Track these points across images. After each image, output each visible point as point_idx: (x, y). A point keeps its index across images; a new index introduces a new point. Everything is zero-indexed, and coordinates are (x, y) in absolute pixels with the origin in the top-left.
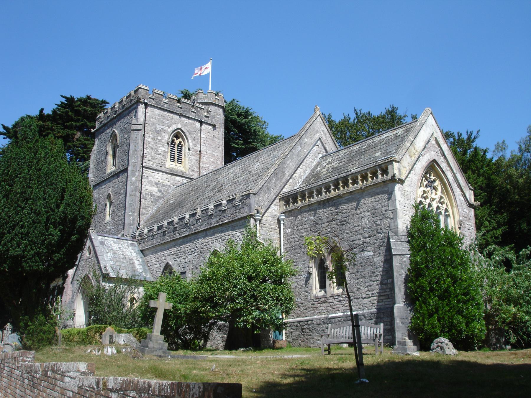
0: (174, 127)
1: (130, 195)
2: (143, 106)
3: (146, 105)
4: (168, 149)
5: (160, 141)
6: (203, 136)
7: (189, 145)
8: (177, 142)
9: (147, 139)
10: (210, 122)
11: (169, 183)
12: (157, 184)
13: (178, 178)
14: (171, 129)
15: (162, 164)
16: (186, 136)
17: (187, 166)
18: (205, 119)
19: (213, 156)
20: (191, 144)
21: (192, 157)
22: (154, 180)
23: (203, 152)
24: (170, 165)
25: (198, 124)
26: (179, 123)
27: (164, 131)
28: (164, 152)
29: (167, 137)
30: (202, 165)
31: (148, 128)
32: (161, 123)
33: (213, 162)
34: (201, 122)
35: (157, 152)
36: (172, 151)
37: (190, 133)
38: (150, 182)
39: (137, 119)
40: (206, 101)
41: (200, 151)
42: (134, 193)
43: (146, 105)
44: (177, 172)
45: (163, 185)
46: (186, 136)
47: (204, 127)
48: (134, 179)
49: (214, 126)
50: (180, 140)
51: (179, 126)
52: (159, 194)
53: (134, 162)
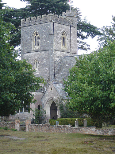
1: (51, 62)
2: (53, 23)
3: (53, 22)
5: (58, 38)
6: (71, 33)
7: (67, 38)
10: (73, 26)
11: (61, 56)
12: (58, 57)
13: (65, 53)
14: (61, 32)
15: (59, 48)
16: (66, 34)
17: (67, 47)
18: (72, 24)
21: (68, 43)
22: (57, 55)
23: (72, 40)
24: (62, 47)
25: (69, 28)
27: (59, 33)
28: (60, 42)
29: (60, 35)
32: (58, 29)
33: (75, 44)
34: (70, 27)
38: (56, 56)
40: (71, 16)
41: (71, 40)
42: (52, 62)
43: (53, 22)
44: (64, 50)
45: (60, 57)
46: (66, 34)
47: (72, 28)
49: (75, 27)
50: (64, 35)
51: (64, 30)
53: (51, 48)
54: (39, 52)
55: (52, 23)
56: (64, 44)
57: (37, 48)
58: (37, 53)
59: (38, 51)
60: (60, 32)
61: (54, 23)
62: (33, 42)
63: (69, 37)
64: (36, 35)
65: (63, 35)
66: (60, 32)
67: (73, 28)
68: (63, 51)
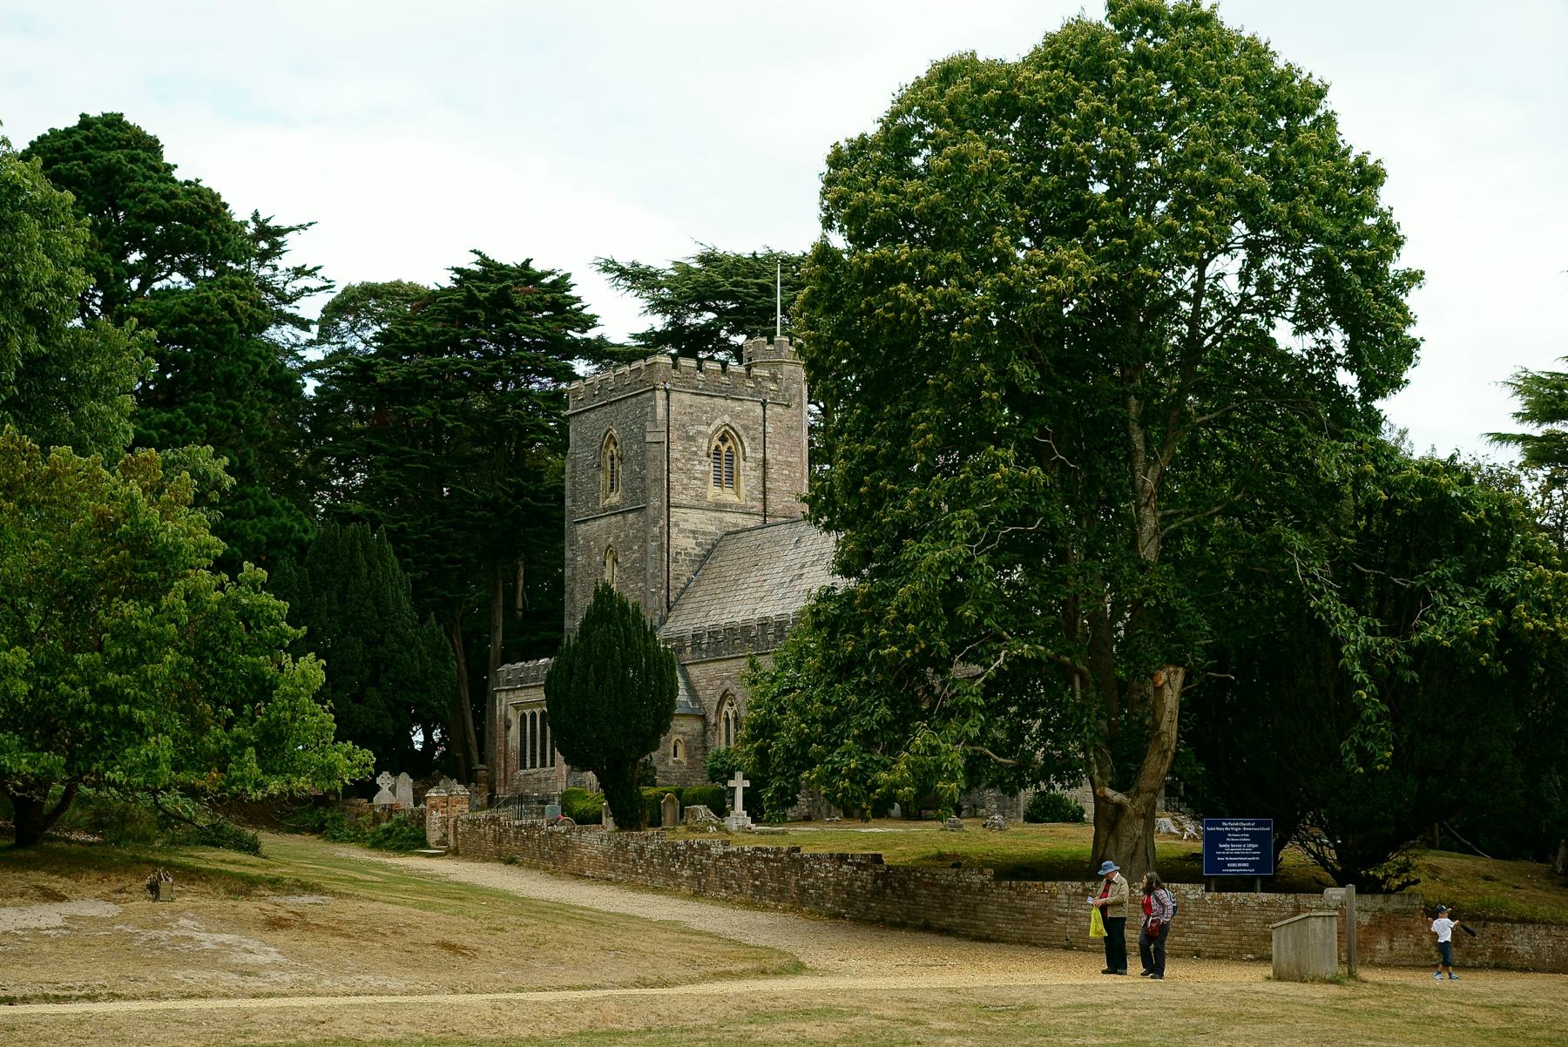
0: (718, 422)
4: (708, 466)
6: (769, 429)
8: (724, 449)
9: (674, 455)
10: (780, 401)
11: (712, 529)
12: (694, 532)
13: (729, 518)
14: (713, 428)
19: (789, 464)
20: (748, 450)
24: (713, 492)
25: (759, 410)
26: (725, 413)
27: (699, 432)
28: (702, 472)
30: (768, 485)
31: (673, 436)
34: (764, 404)
35: (688, 473)
36: (718, 468)
37: (746, 428)
38: (681, 531)
39: (654, 420)
45: (704, 533)
48: (656, 530)
50: (730, 443)
51: (727, 419)
52: (698, 550)
54: (620, 517)
55: (660, 395)
56: (727, 477)
57: (615, 498)
58: (613, 519)
59: (613, 511)
60: (702, 428)
61: (673, 395)
62: (602, 476)
63: (754, 450)
64: (612, 447)
65: (723, 439)
66: (702, 428)
67: (779, 410)
68: (720, 507)
